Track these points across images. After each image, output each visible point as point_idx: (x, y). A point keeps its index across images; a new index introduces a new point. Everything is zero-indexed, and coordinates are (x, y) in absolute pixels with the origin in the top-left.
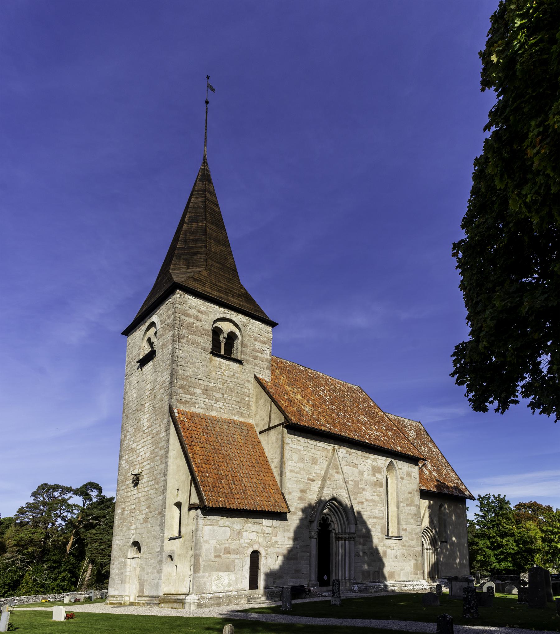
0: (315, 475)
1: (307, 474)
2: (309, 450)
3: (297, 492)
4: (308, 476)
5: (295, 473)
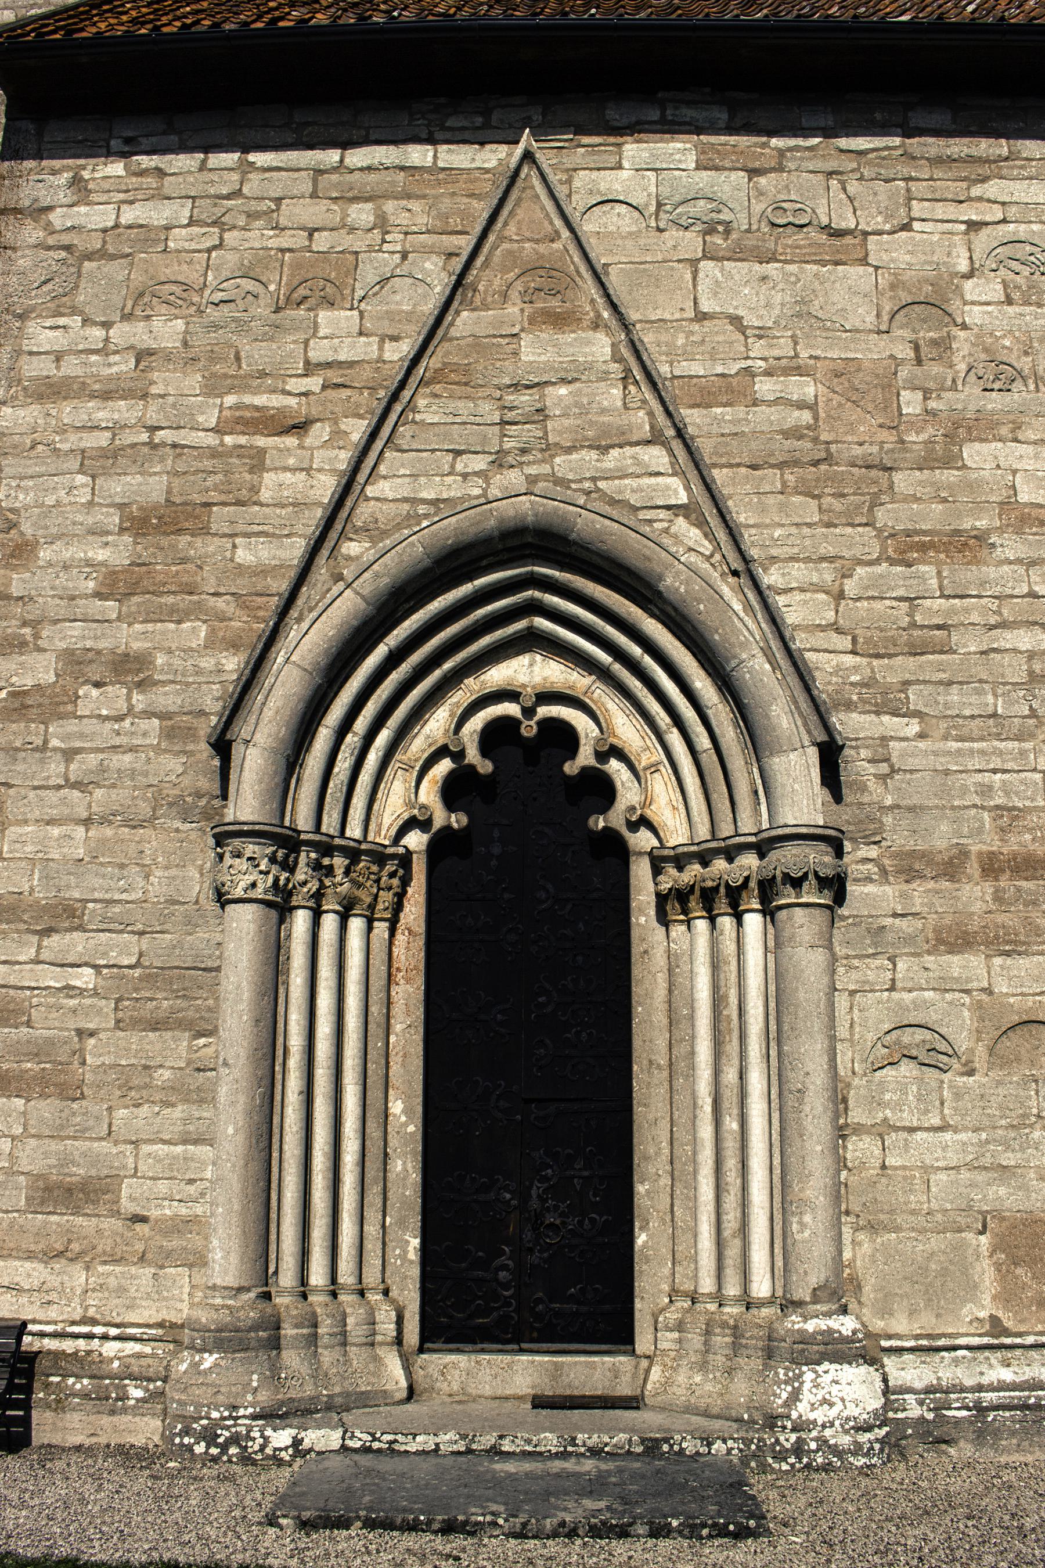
0: (314, 383)
1: (213, 388)
2: (252, 216)
3: (97, 531)
4: (230, 400)
5: (92, 396)
